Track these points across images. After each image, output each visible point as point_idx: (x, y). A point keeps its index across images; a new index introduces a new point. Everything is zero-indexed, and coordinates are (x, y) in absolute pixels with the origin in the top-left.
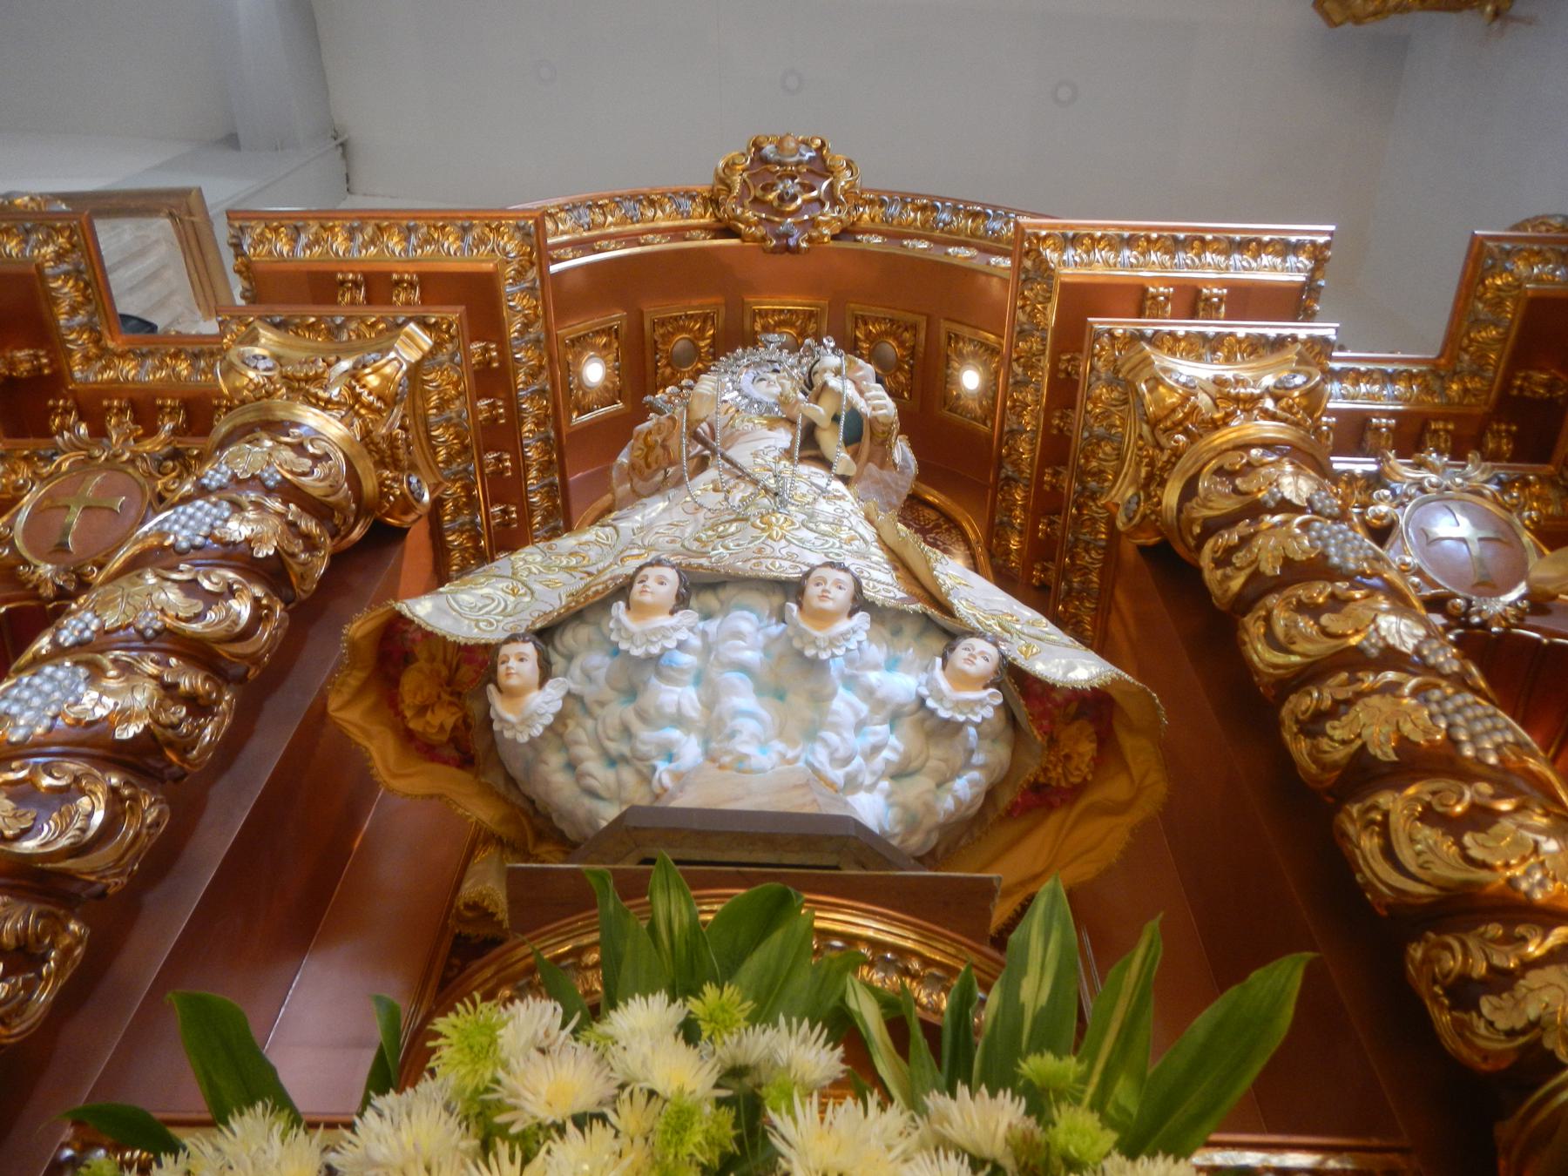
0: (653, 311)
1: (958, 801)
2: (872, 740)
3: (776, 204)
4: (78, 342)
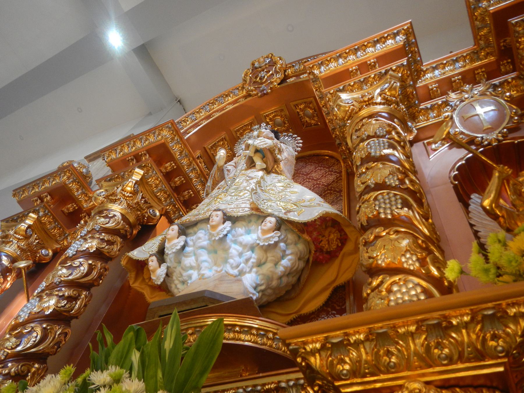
1: (284, 267)
2: (245, 257)
3: (259, 81)
4: (82, 198)
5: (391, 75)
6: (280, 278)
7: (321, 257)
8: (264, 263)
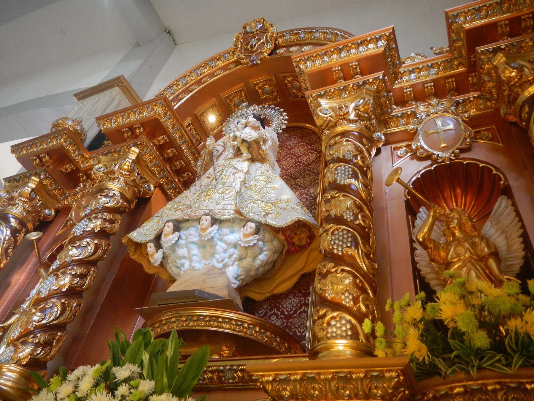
0: (224, 94)
1: (261, 261)
2: (229, 254)
4: (78, 159)
5: (367, 89)
6: (258, 269)
7: (293, 249)
8: (245, 258)
